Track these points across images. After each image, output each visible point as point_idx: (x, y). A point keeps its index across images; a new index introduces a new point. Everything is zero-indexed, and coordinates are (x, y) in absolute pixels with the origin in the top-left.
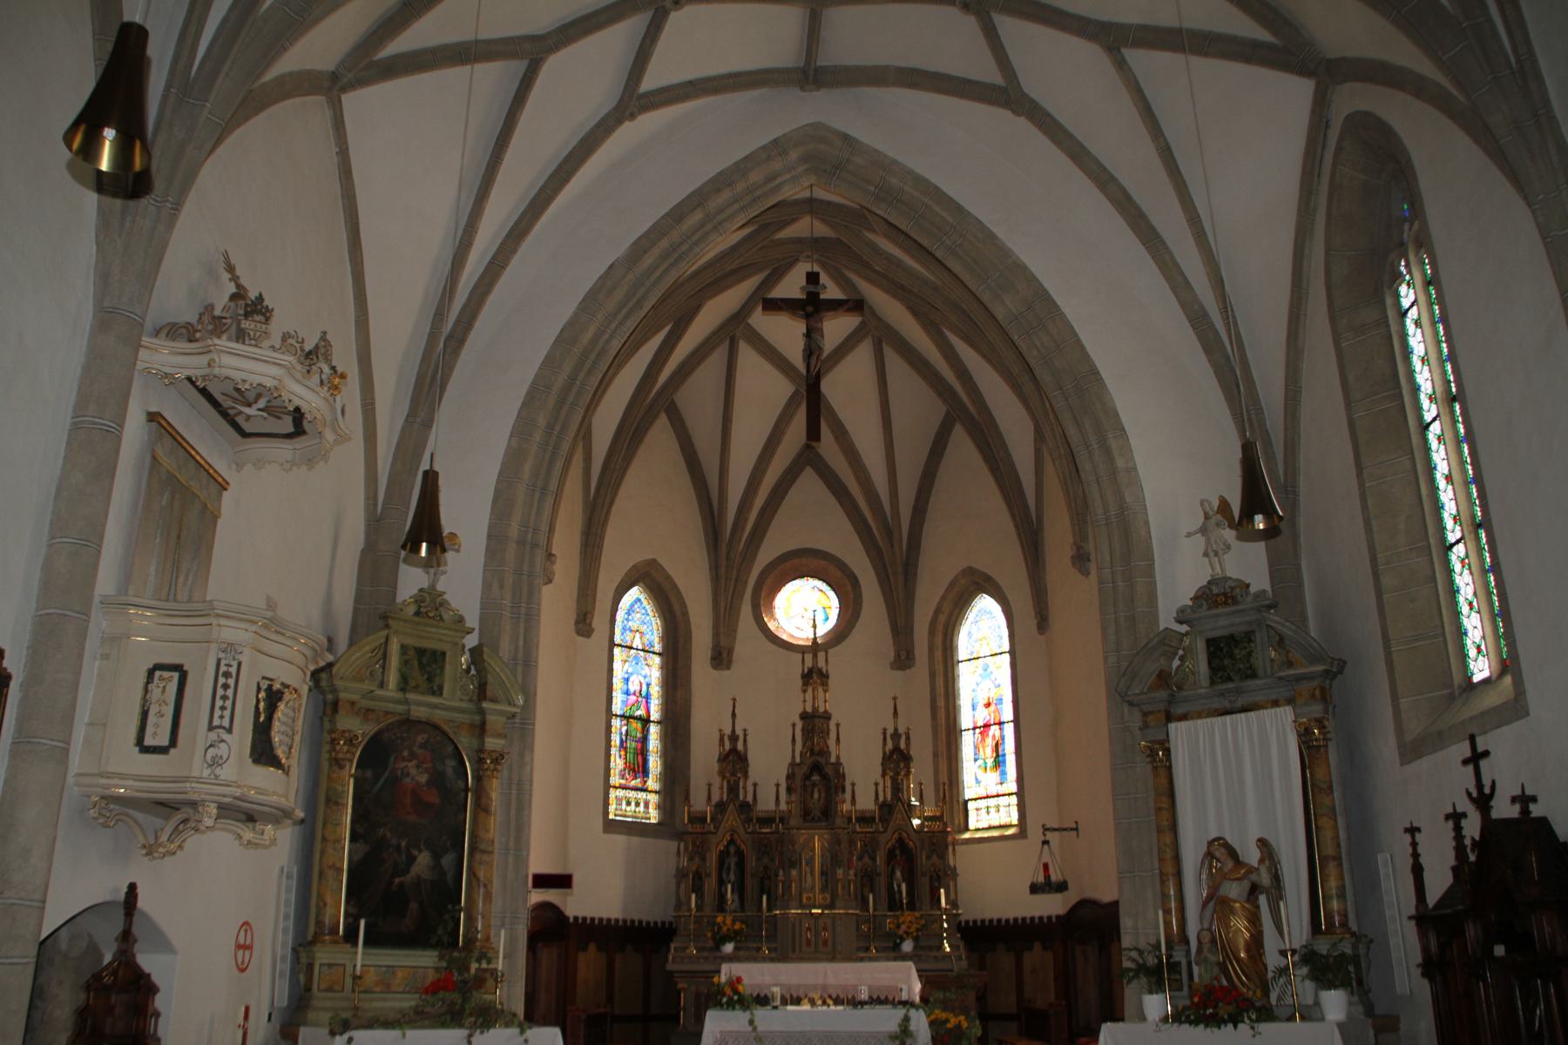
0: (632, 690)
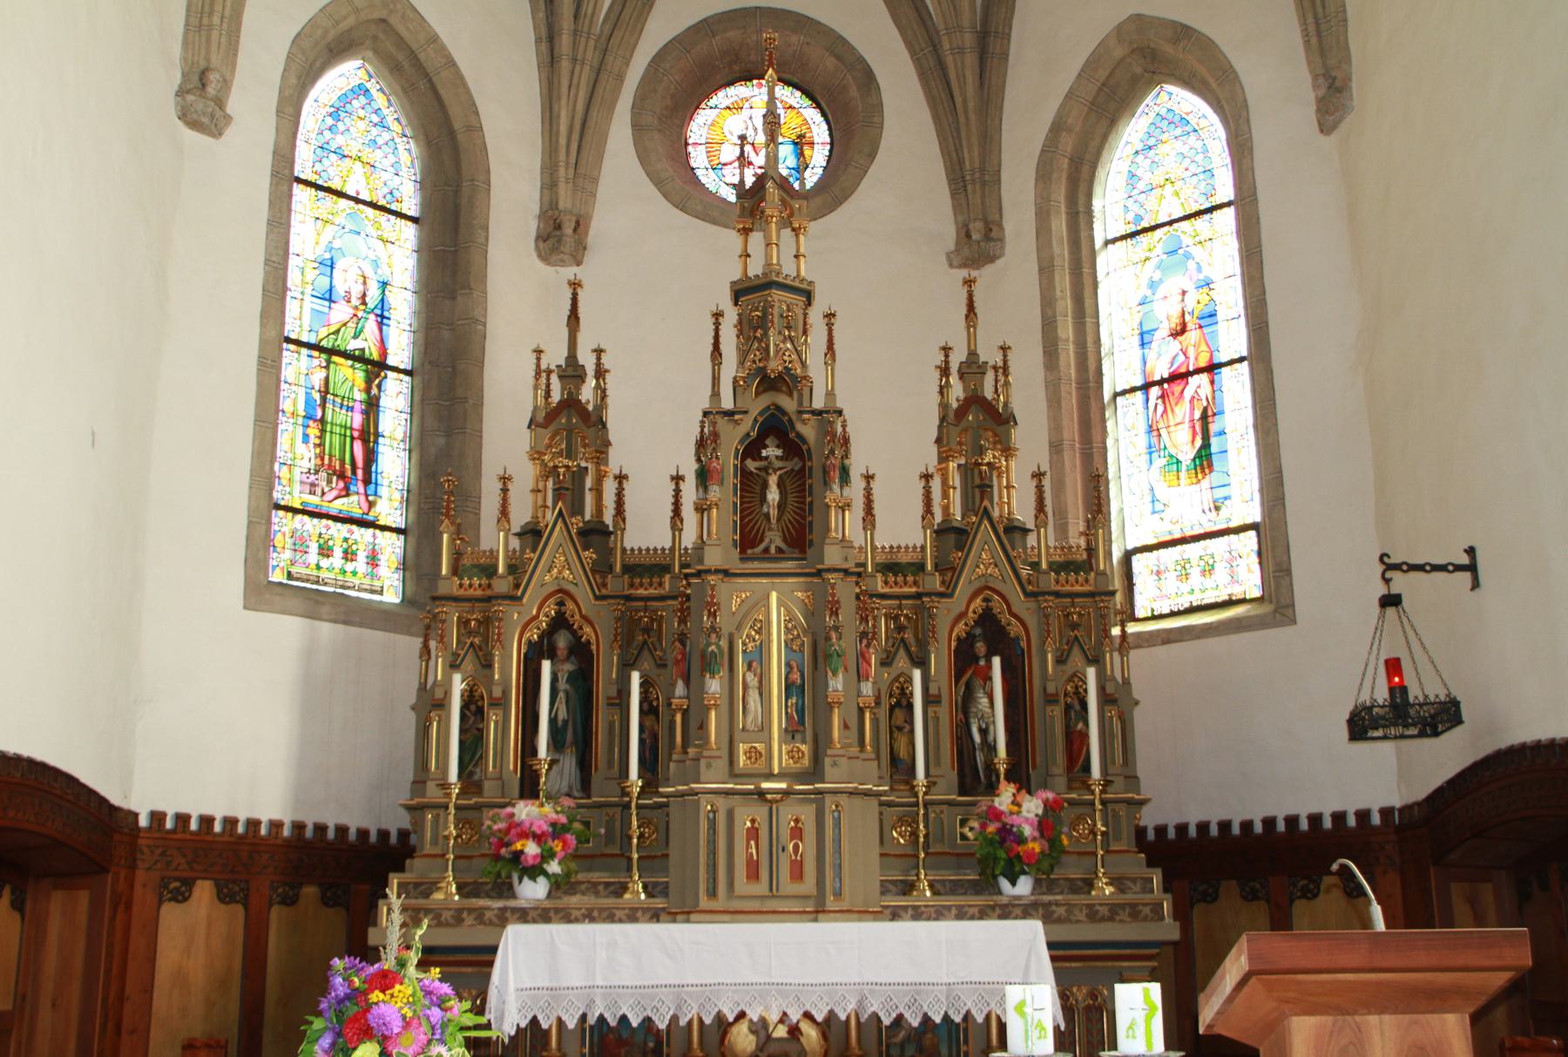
0: (340, 289)
